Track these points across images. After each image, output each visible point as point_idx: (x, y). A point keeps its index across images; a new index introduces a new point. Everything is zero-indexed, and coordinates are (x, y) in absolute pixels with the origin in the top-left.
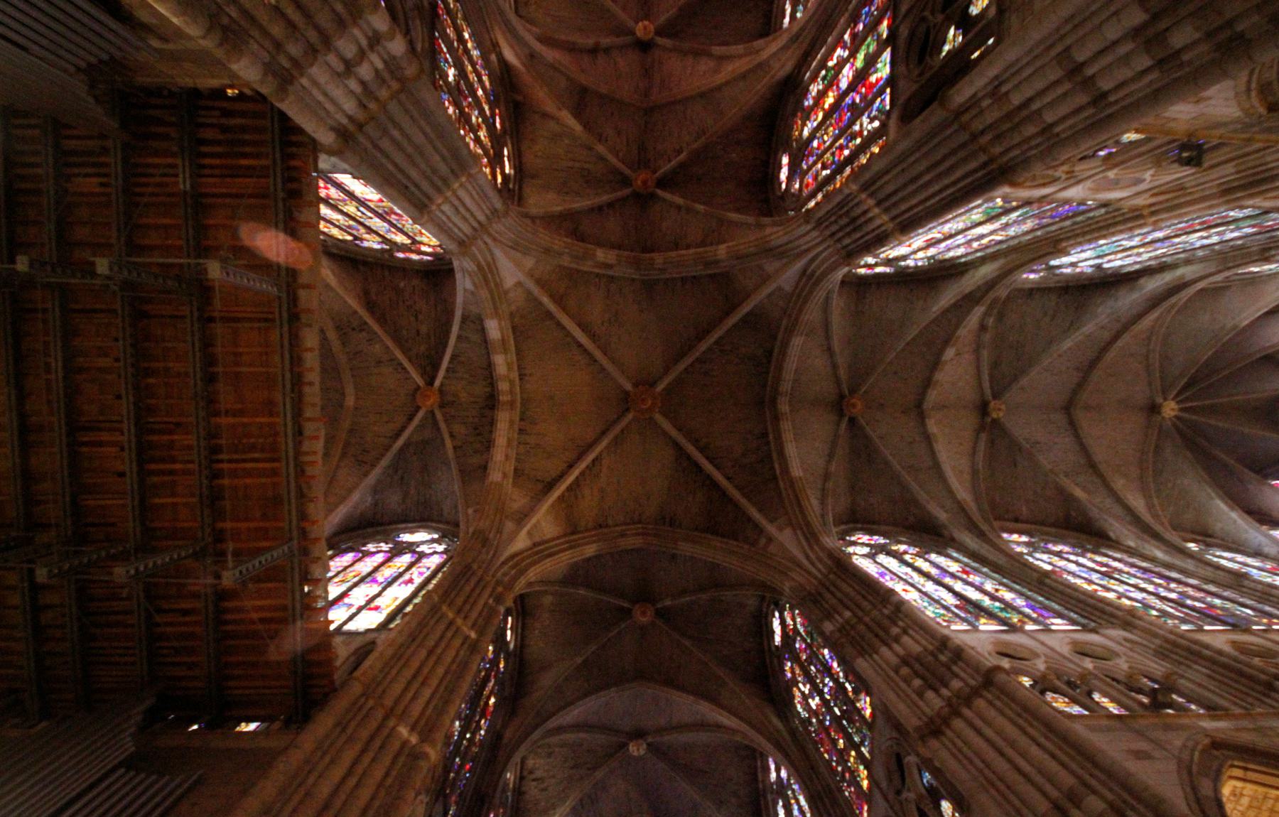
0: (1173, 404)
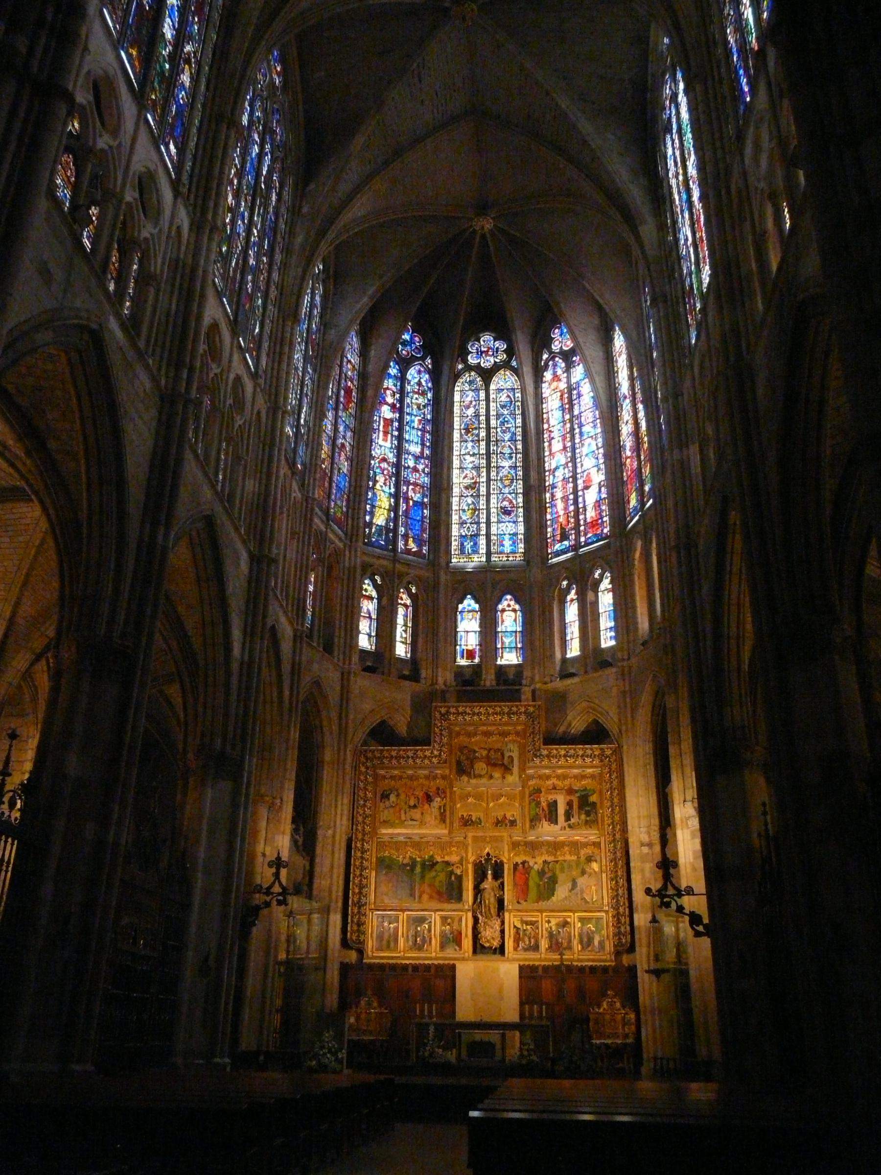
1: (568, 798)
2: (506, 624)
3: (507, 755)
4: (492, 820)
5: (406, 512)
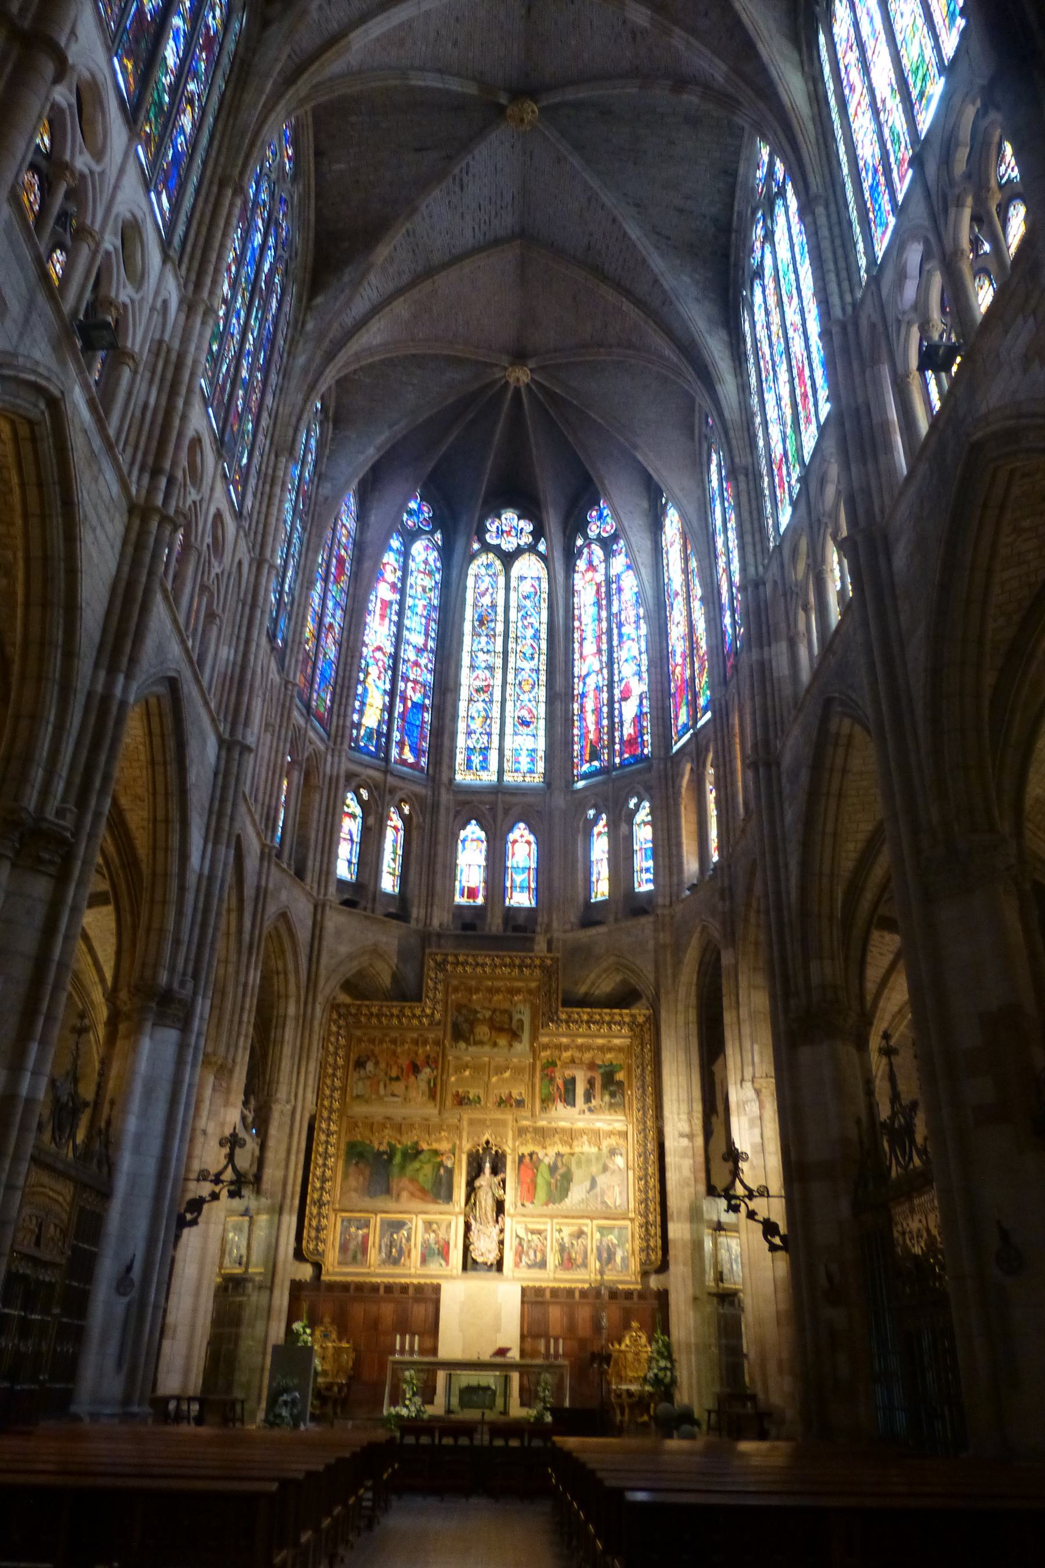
1: (589, 1074)
3: (516, 1017)
4: (493, 1099)
5: (403, 716)
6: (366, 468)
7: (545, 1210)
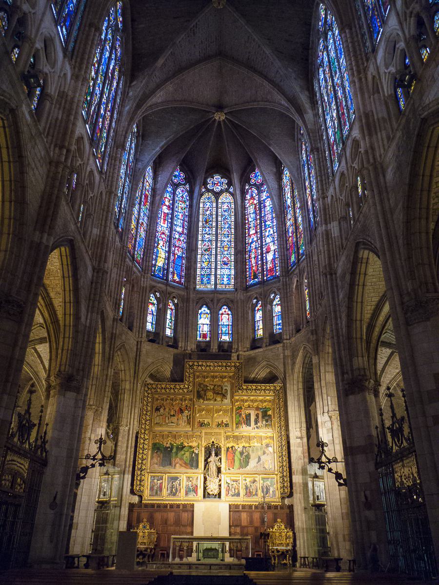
0: (223, 118)
1: (257, 412)
2: (224, 320)
4: (215, 423)
5: (174, 261)
6: (156, 156)
7: (238, 471)
